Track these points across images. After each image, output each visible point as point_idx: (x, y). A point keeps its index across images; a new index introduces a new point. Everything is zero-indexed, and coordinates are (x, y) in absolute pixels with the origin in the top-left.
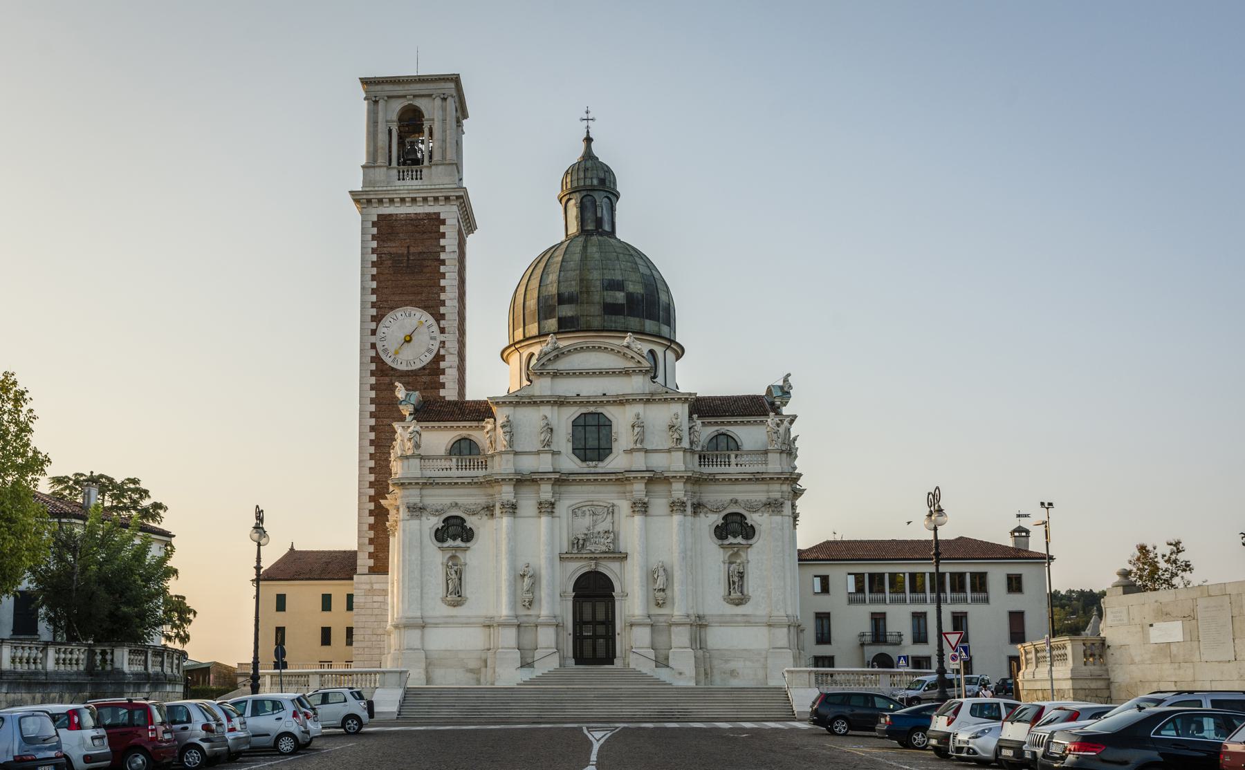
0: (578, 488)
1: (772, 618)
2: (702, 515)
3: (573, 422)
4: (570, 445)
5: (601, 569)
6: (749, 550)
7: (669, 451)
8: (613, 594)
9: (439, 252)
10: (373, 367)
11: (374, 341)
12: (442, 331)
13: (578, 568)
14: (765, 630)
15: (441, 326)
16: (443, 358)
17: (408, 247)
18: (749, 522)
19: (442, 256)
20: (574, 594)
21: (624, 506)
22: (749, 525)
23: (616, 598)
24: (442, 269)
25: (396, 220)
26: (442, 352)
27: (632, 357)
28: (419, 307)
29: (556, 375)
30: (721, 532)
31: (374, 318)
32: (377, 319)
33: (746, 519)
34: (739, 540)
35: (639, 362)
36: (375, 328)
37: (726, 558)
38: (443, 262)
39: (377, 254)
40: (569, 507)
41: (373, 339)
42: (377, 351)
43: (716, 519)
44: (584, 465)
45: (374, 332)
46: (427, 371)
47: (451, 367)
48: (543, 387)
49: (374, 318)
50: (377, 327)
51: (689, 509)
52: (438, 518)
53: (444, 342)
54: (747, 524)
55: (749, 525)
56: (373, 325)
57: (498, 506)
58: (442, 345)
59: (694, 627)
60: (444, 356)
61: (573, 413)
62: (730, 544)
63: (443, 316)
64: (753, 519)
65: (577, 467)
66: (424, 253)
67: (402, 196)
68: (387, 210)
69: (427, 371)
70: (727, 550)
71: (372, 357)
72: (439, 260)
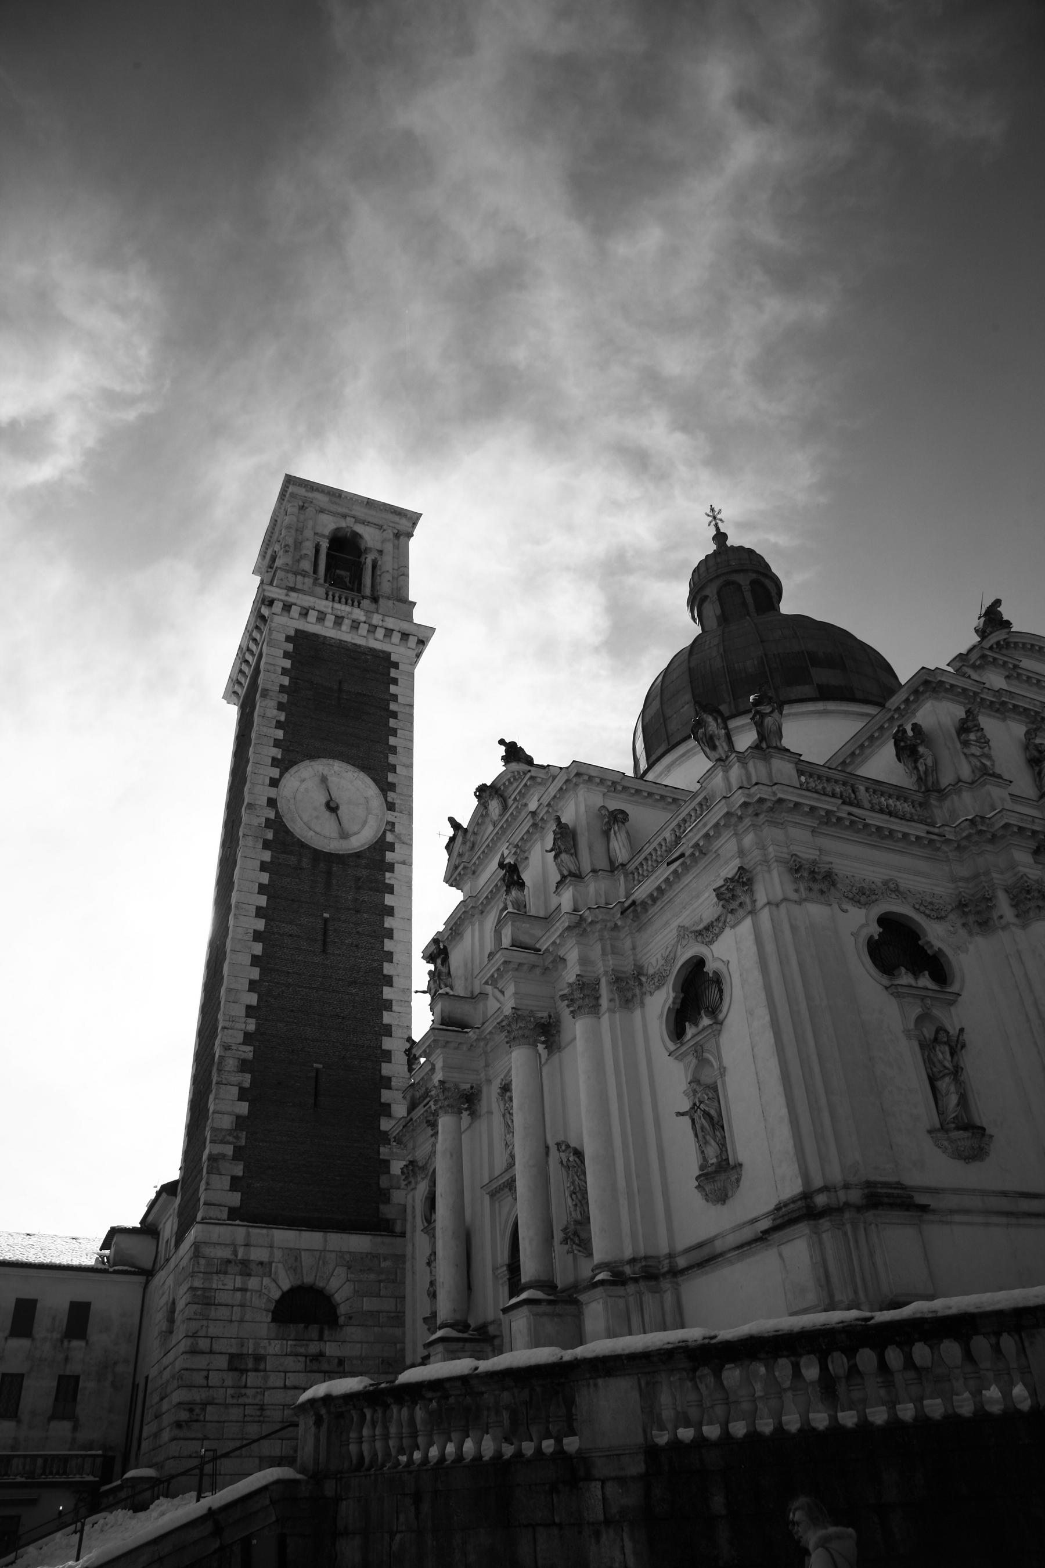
9: (388, 701)
10: (270, 835)
11: (273, 795)
12: (391, 807)
15: (389, 799)
16: (391, 847)
17: (340, 683)
19: (393, 707)
24: (392, 723)
25: (324, 643)
26: (389, 837)
28: (353, 765)
31: (275, 762)
32: (284, 764)
36: (277, 776)
38: (394, 715)
39: (290, 677)
41: (272, 792)
42: (277, 814)
45: (274, 783)
46: (364, 862)
47: (404, 863)
49: (275, 762)
50: (281, 775)
53: (393, 824)
56: (275, 773)
58: (389, 828)
60: (393, 844)
63: (392, 787)
66: (364, 695)
67: (339, 614)
68: (311, 626)
69: (364, 862)
71: (267, 820)
72: (387, 710)
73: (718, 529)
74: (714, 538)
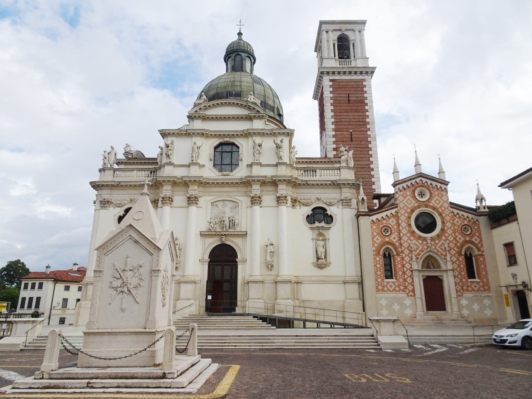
0: (216, 189)
1: (347, 278)
2: (298, 207)
3: (216, 148)
4: (212, 163)
5: (228, 243)
6: (329, 230)
7: (276, 165)
8: (237, 260)
13: (213, 242)
14: (342, 287)
18: (329, 213)
20: (209, 260)
21: (245, 201)
22: (329, 215)
23: (238, 263)
27: (254, 109)
29: (205, 118)
30: (311, 219)
33: (326, 211)
34: (323, 224)
35: (258, 111)
37: (315, 237)
40: (209, 201)
43: (308, 210)
44: (221, 174)
48: (198, 125)
51: (289, 203)
52: (120, 208)
54: (327, 214)
55: (329, 215)
57: (160, 199)
59: (293, 284)
61: (216, 142)
62: (318, 227)
64: (330, 211)
65: (216, 175)
70: (314, 231)
73: (240, 31)
74: (238, 34)
